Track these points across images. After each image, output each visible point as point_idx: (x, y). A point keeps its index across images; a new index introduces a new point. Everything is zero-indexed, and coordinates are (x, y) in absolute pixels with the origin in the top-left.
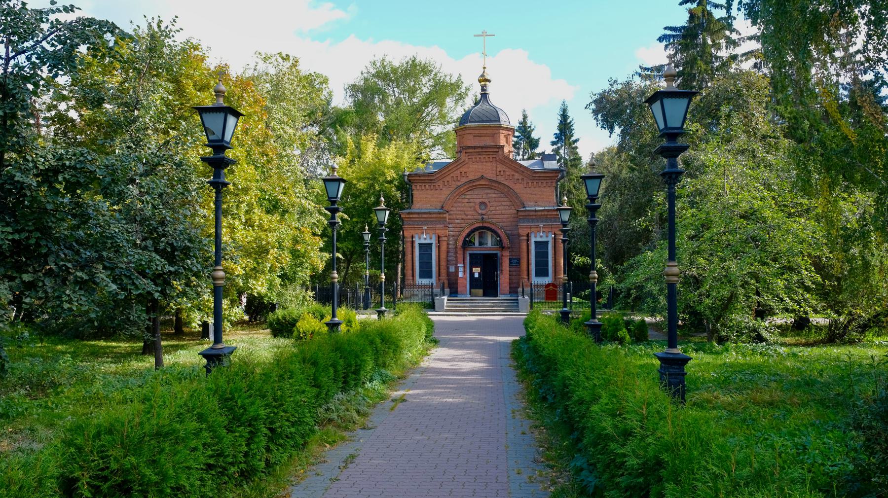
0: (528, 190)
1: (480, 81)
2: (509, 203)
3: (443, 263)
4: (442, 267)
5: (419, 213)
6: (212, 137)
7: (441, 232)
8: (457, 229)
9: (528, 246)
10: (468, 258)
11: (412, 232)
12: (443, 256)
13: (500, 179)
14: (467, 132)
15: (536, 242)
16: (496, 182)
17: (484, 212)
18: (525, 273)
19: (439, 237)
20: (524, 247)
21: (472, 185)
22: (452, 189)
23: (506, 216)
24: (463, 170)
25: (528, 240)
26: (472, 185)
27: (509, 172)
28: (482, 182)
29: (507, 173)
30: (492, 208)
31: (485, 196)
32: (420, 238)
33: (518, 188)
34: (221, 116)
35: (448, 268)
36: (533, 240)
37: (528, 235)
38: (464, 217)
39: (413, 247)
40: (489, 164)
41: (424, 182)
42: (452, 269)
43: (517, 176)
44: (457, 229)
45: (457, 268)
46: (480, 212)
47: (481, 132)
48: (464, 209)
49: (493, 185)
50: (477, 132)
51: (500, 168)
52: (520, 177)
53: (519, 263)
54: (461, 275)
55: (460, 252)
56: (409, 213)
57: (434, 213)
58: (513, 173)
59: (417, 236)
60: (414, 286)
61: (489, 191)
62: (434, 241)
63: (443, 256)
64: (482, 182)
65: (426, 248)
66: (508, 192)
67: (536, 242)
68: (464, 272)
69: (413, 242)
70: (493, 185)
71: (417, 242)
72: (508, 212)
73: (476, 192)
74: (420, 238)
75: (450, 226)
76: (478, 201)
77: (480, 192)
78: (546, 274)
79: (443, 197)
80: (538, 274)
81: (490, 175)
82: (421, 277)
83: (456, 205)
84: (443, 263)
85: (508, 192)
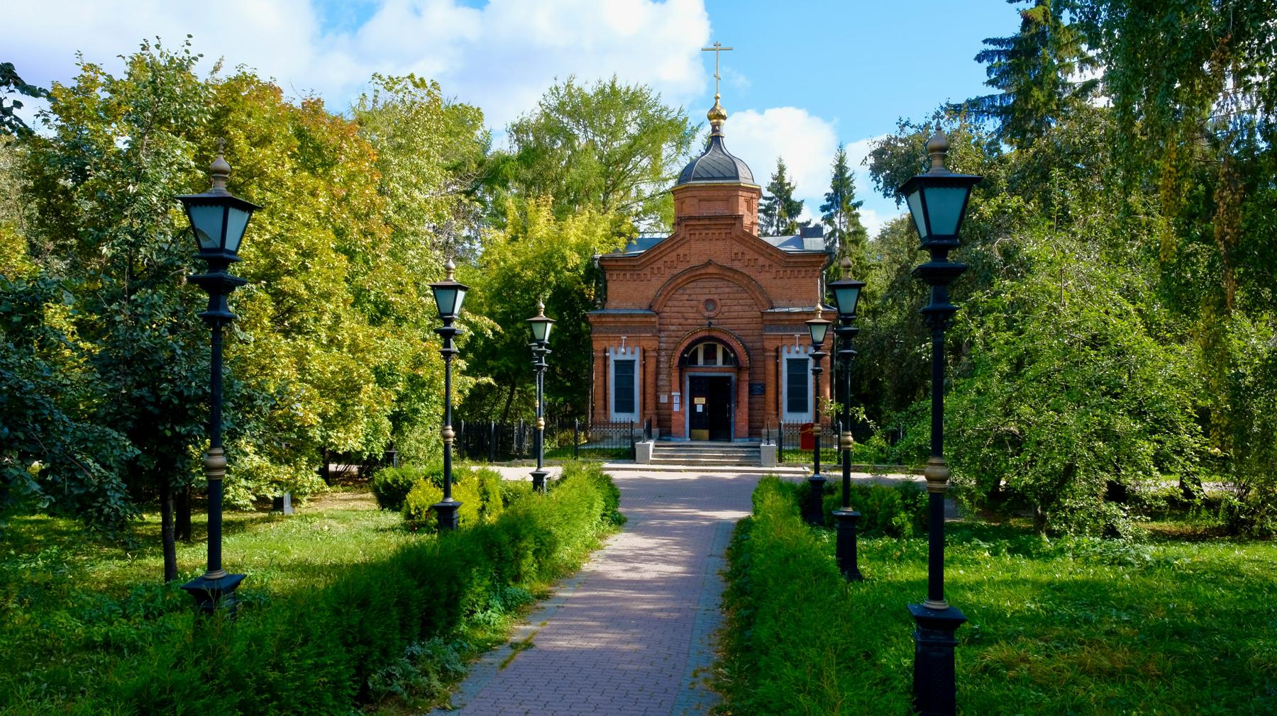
0: (779, 282)
1: (710, 118)
2: (750, 302)
3: (650, 390)
4: (648, 396)
5: (614, 316)
6: (205, 244)
8: (671, 340)
9: (777, 365)
10: (688, 383)
11: (605, 344)
12: (650, 380)
13: (737, 265)
14: (689, 194)
15: (789, 361)
16: (730, 269)
17: (712, 314)
18: (773, 406)
19: (644, 351)
20: (771, 367)
22: (665, 280)
23: (744, 321)
24: (681, 251)
25: (777, 357)
26: (695, 274)
27: (750, 255)
28: (711, 270)
29: (747, 257)
30: (725, 309)
31: (713, 290)
32: (616, 353)
33: (765, 279)
34: (219, 211)
35: (657, 397)
36: (785, 356)
37: (777, 350)
38: (681, 321)
39: (605, 366)
40: (720, 243)
41: (623, 268)
42: (664, 399)
43: (761, 260)
44: (671, 340)
45: (670, 397)
46: (707, 314)
47: (711, 193)
48: (683, 309)
49: (726, 273)
50: (704, 194)
51: (737, 248)
52: (767, 263)
53: (763, 392)
54: (676, 408)
55: (676, 375)
56: (600, 316)
57: (638, 315)
58: (756, 256)
59: (612, 350)
60: (607, 424)
61: (720, 284)
62: (637, 357)
63: (650, 380)
64: (711, 270)
65: (625, 368)
66: (746, 284)
67: (789, 361)
68: (682, 403)
69: (605, 359)
70: (726, 273)
71: (612, 357)
72: (748, 314)
73: (701, 284)
74: (616, 353)
75: (662, 334)
76: (703, 298)
77: (707, 284)
78: (803, 408)
79: (651, 293)
80: (791, 409)
81: (722, 260)
82: (617, 410)
83: (670, 303)
84: (650, 390)
85: (746, 284)
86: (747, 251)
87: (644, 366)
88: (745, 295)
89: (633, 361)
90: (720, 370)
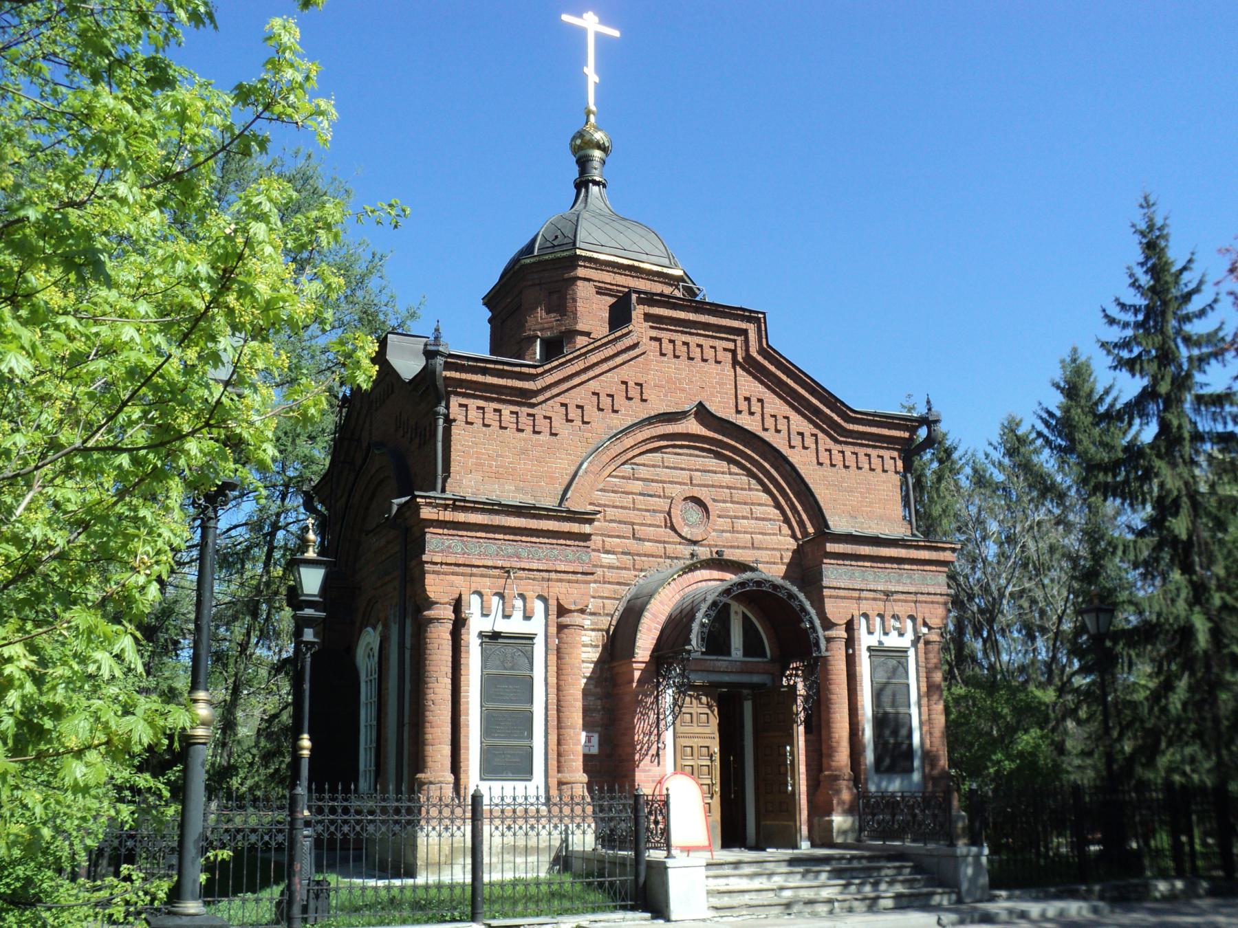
7: (569, 594)
9: (851, 661)
11: (460, 584)
21: (663, 431)
26: (663, 431)
40: (711, 367)
48: (633, 516)
49: (727, 439)
58: (786, 410)
61: (712, 463)
62: (536, 626)
64: (692, 426)
71: (477, 624)
73: (671, 459)
79: (562, 467)
81: (721, 408)
86: (768, 396)
87: (559, 654)
88: (765, 497)
89: (530, 638)
90: (745, 669)
